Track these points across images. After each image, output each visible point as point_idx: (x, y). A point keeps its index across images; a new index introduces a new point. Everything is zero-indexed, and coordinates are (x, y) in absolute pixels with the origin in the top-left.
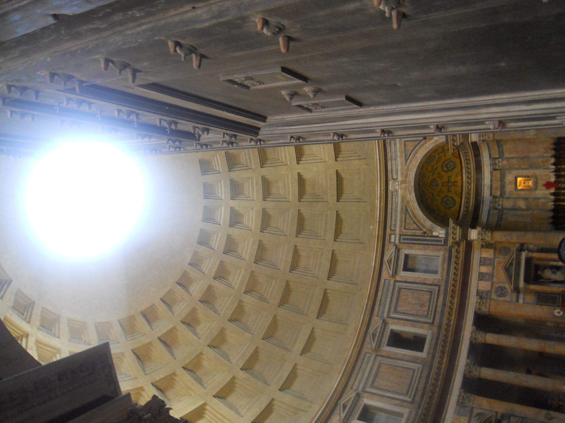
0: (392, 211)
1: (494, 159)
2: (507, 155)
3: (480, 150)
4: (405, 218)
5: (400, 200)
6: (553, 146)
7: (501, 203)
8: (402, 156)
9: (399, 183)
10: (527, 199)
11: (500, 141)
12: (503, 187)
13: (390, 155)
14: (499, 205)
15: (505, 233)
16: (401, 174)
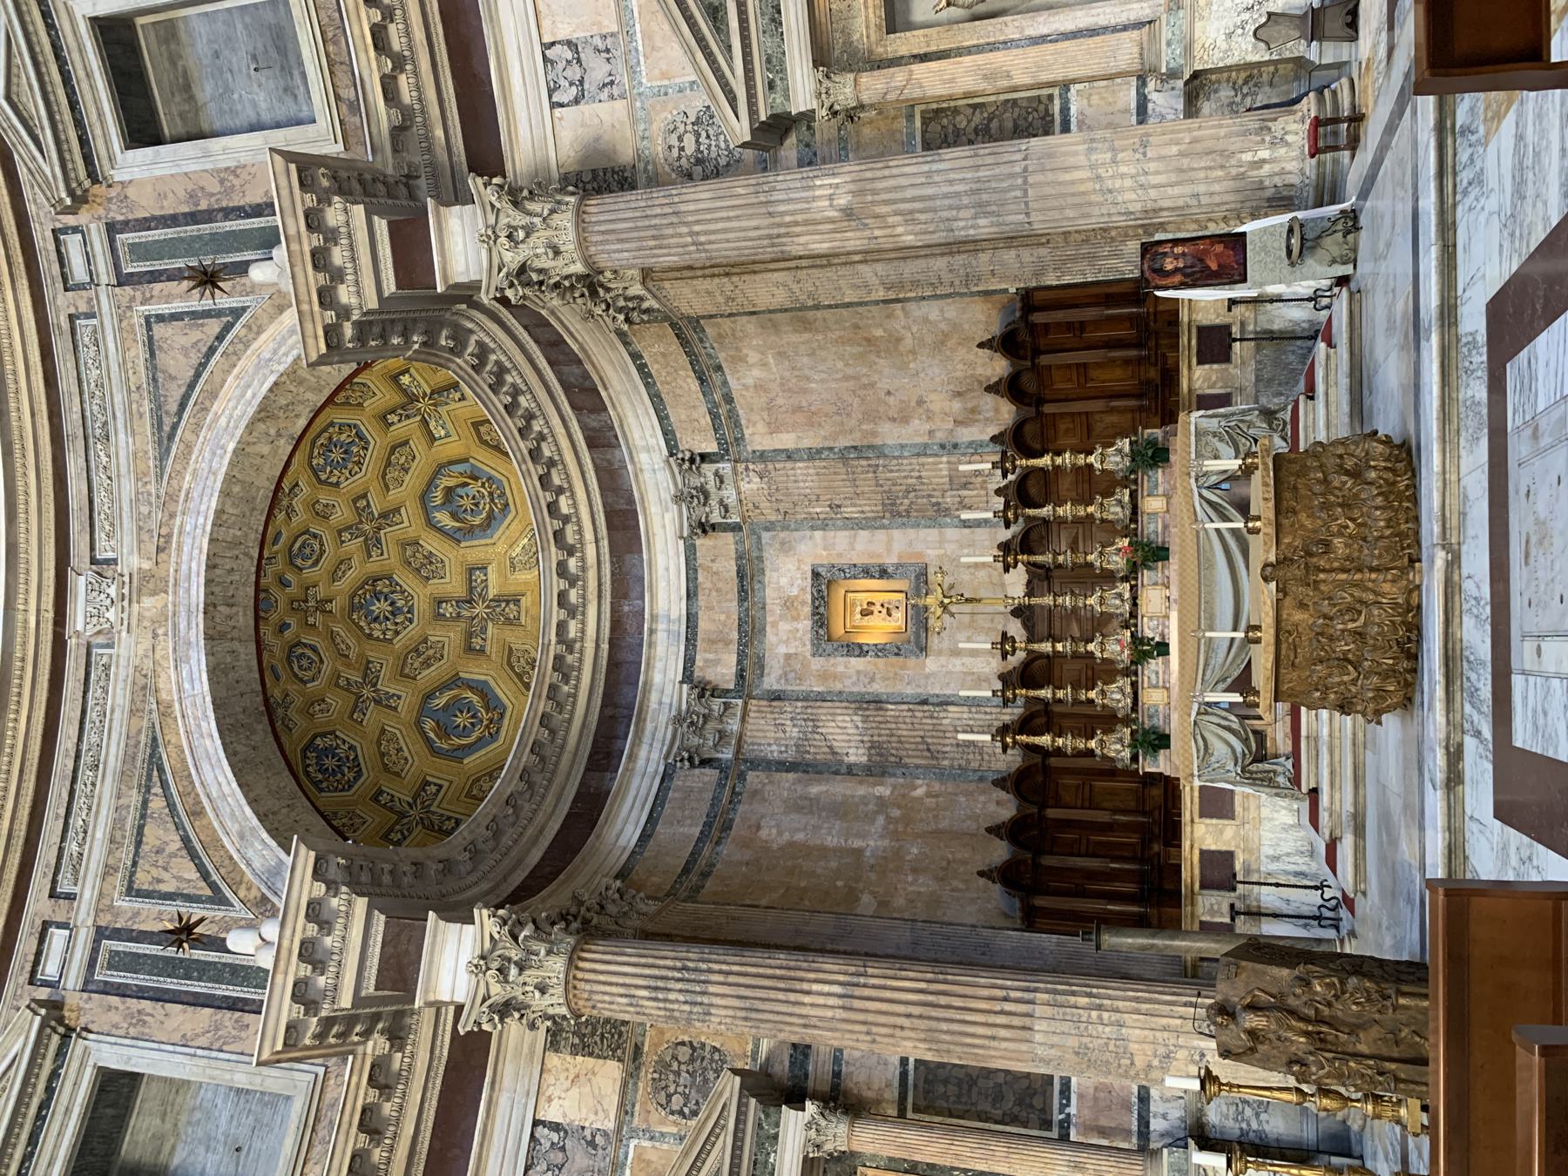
0: (75, 771)
1: (692, 461)
2: (758, 437)
3: (603, 394)
4: (143, 816)
5: (119, 696)
6: (999, 367)
7: (733, 725)
8: (141, 416)
9: (126, 591)
10: (877, 702)
11: (696, 322)
12: (750, 631)
13: (76, 408)
14: (722, 734)
15: (667, 958)
16: (140, 528)
